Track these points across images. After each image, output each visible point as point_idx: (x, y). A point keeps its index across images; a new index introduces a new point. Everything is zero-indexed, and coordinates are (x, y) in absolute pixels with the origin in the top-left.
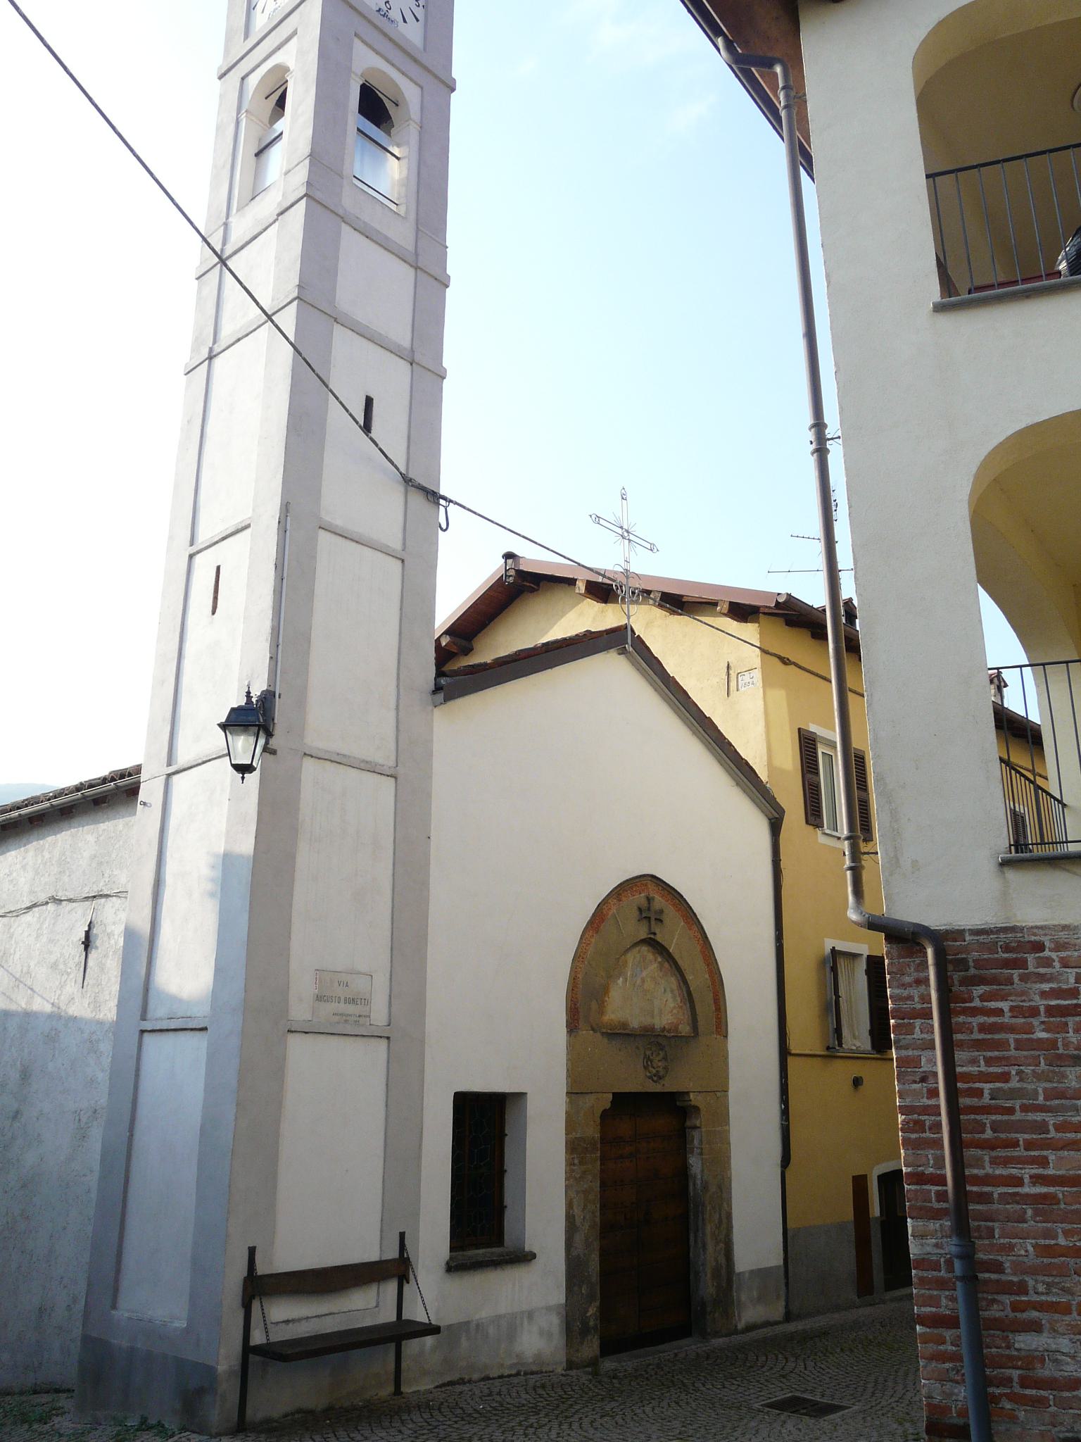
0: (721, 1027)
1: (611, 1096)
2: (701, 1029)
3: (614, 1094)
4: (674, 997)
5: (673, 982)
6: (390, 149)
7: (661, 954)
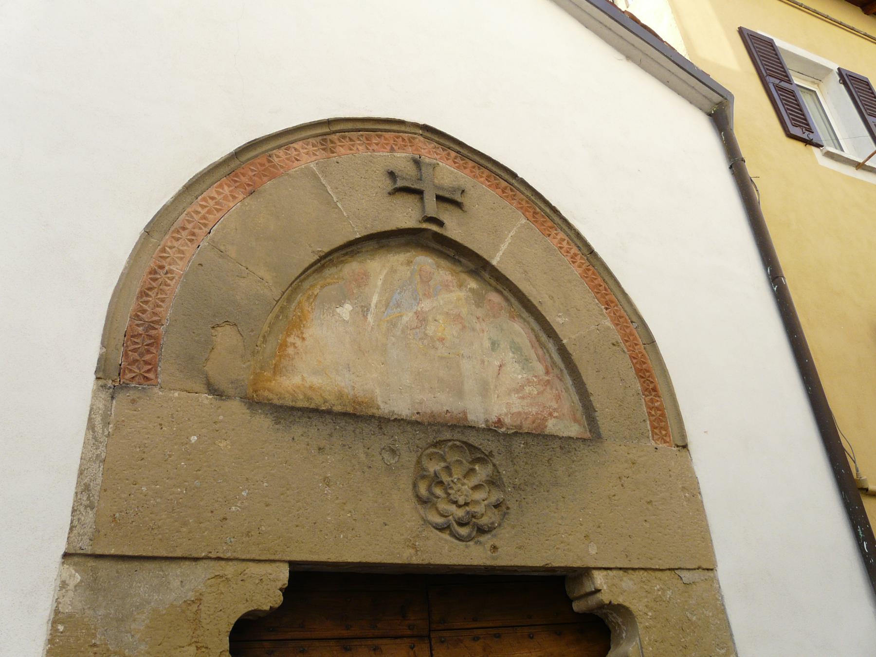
0: (661, 417)
1: (283, 575)
2: (605, 425)
3: (292, 564)
4: (525, 362)
5: (520, 330)
6: (213, 580)
7: (474, 273)
